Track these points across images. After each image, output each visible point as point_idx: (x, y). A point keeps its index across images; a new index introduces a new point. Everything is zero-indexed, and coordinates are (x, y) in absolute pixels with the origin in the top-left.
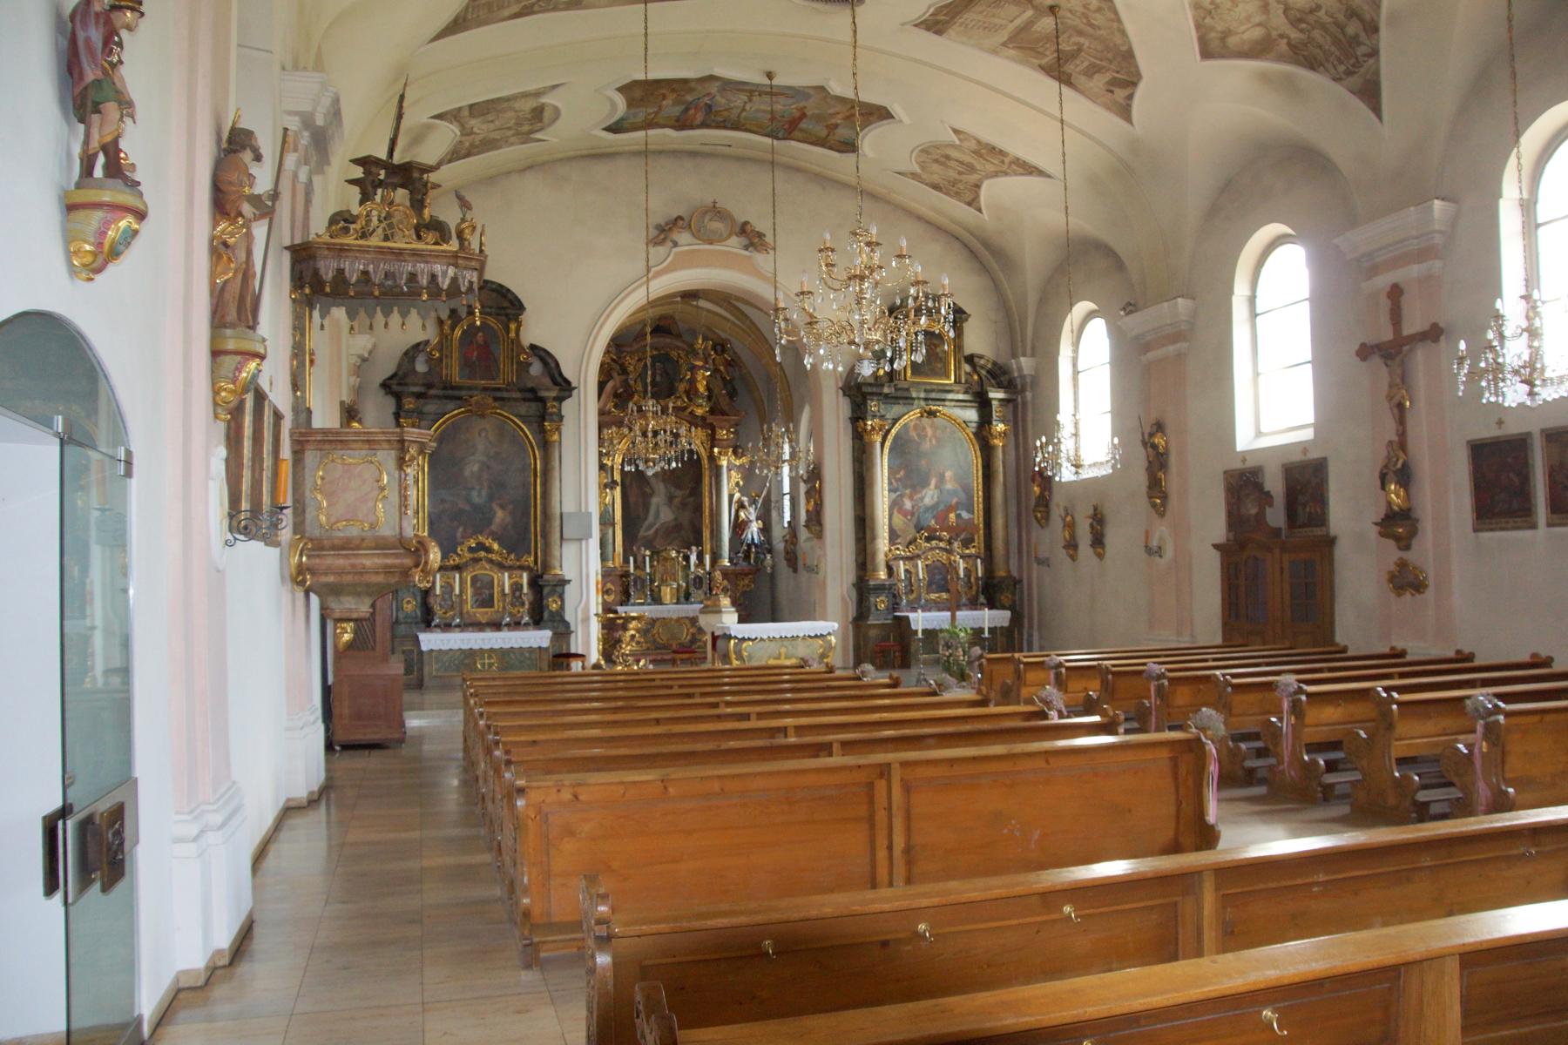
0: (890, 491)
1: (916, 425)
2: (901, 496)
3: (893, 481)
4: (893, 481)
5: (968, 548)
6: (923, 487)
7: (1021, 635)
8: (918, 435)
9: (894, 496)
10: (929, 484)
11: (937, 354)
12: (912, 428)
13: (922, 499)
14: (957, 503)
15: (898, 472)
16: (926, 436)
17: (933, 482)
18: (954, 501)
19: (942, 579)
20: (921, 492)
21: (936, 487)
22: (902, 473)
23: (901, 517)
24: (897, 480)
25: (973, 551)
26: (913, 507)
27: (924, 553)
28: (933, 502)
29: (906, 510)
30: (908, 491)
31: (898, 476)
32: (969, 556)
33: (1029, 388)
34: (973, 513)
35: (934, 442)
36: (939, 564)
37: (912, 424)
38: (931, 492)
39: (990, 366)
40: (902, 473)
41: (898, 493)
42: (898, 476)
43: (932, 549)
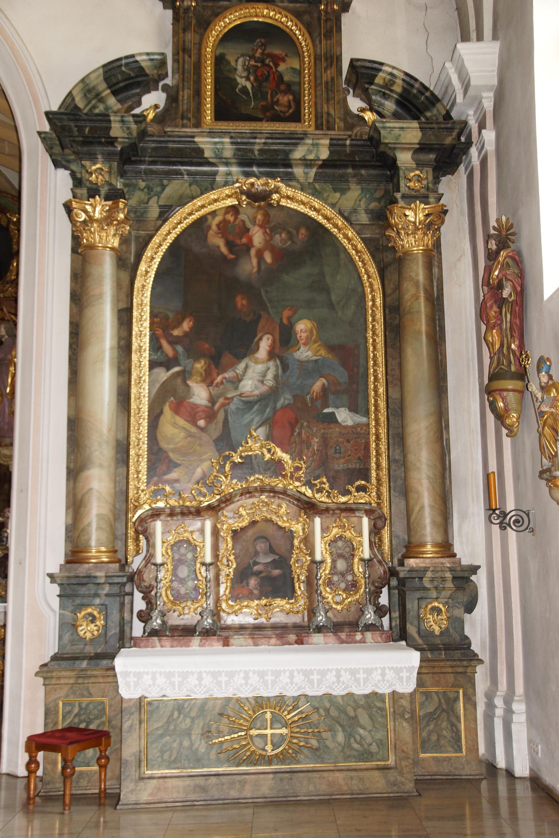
0: (153, 365)
1: (223, 227)
2: (184, 375)
3: (164, 343)
4: (164, 343)
5: (346, 493)
6: (240, 357)
7: (470, 701)
8: (230, 245)
9: (163, 375)
10: (257, 348)
11: (281, 76)
12: (214, 227)
13: (237, 381)
14: (324, 389)
15: (179, 324)
16: (249, 246)
17: (265, 344)
18: (318, 385)
19: (275, 564)
20: (232, 365)
21: (271, 355)
22: (186, 325)
23: (181, 422)
24: (173, 342)
25: (362, 498)
26: (212, 400)
27: (227, 500)
28: (264, 389)
29: (196, 406)
30: (200, 365)
31: (176, 332)
32: (349, 509)
33: (489, 122)
34: (367, 413)
35: (268, 257)
36: (270, 531)
37: (218, 219)
38: (260, 368)
39: (398, 88)
40: (186, 325)
41: (176, 369)
42: (176, 332)
43: (247, 492)
